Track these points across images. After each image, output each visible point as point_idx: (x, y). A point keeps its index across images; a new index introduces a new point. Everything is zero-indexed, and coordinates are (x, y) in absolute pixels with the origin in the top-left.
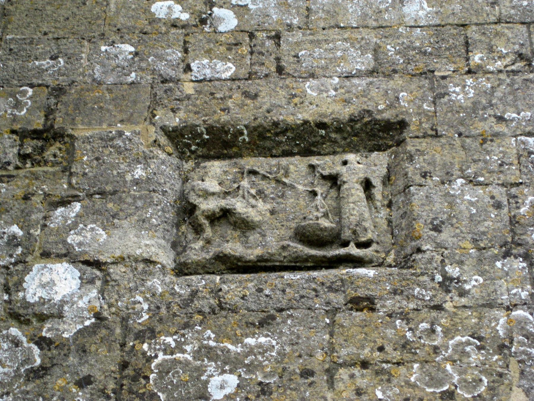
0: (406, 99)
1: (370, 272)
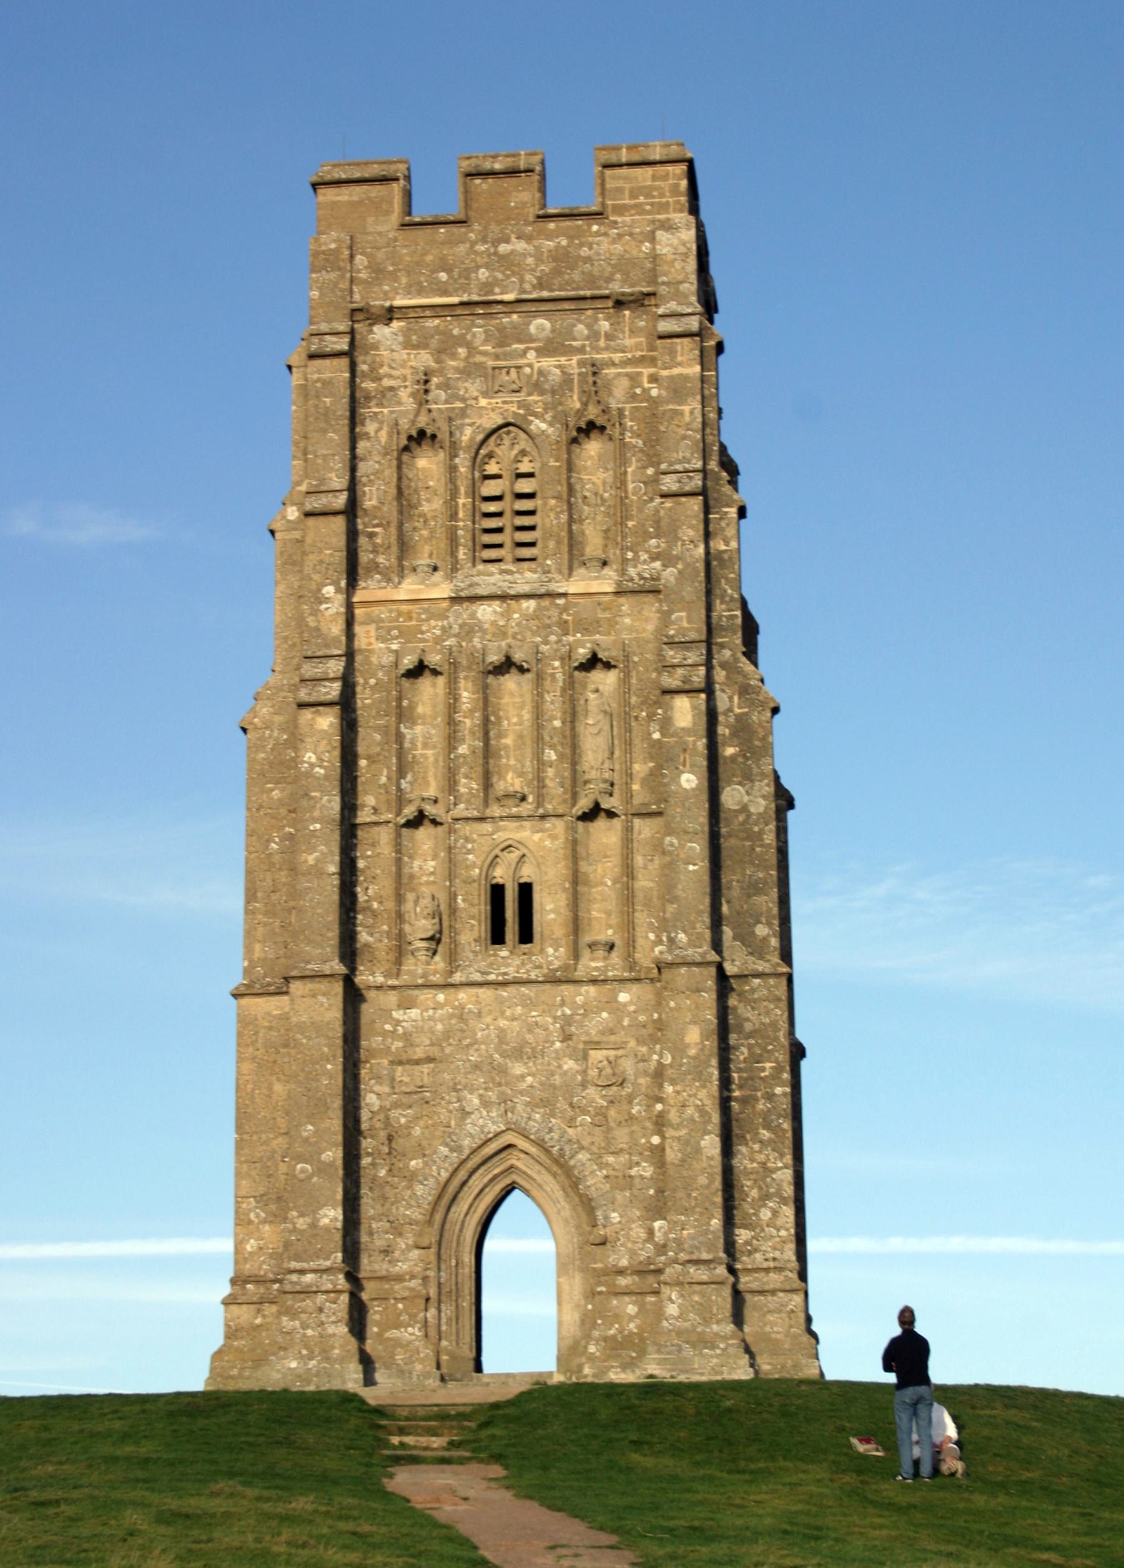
0: (435, 1052)
1: (428, 1094)
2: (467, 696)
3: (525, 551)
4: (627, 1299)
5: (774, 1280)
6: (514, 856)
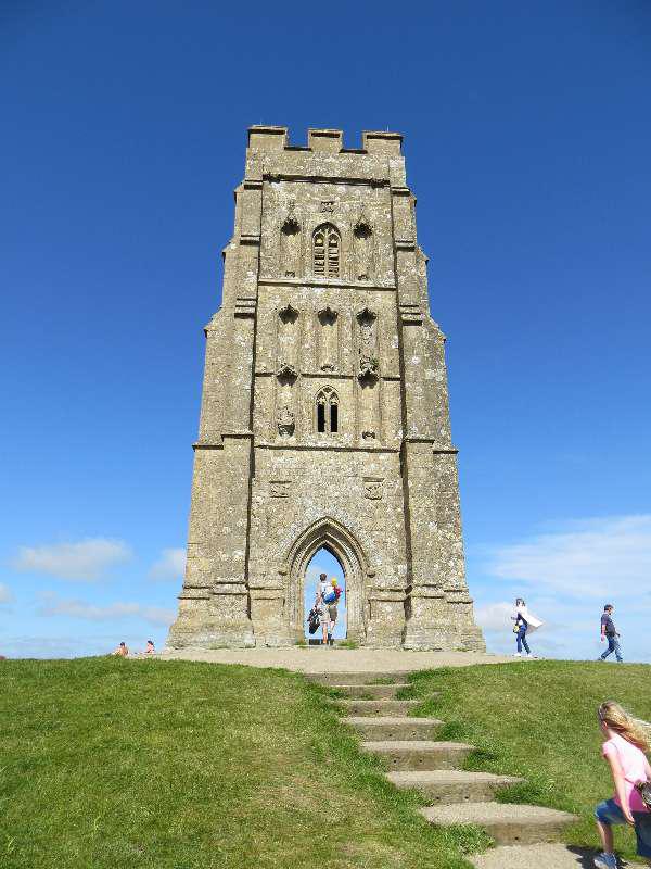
2: (309, 324)
3: (335, 272)
4: (386, 604)
5: (457, 597)
6: (328, 395)
